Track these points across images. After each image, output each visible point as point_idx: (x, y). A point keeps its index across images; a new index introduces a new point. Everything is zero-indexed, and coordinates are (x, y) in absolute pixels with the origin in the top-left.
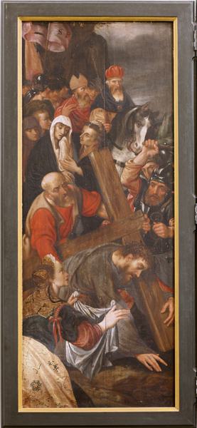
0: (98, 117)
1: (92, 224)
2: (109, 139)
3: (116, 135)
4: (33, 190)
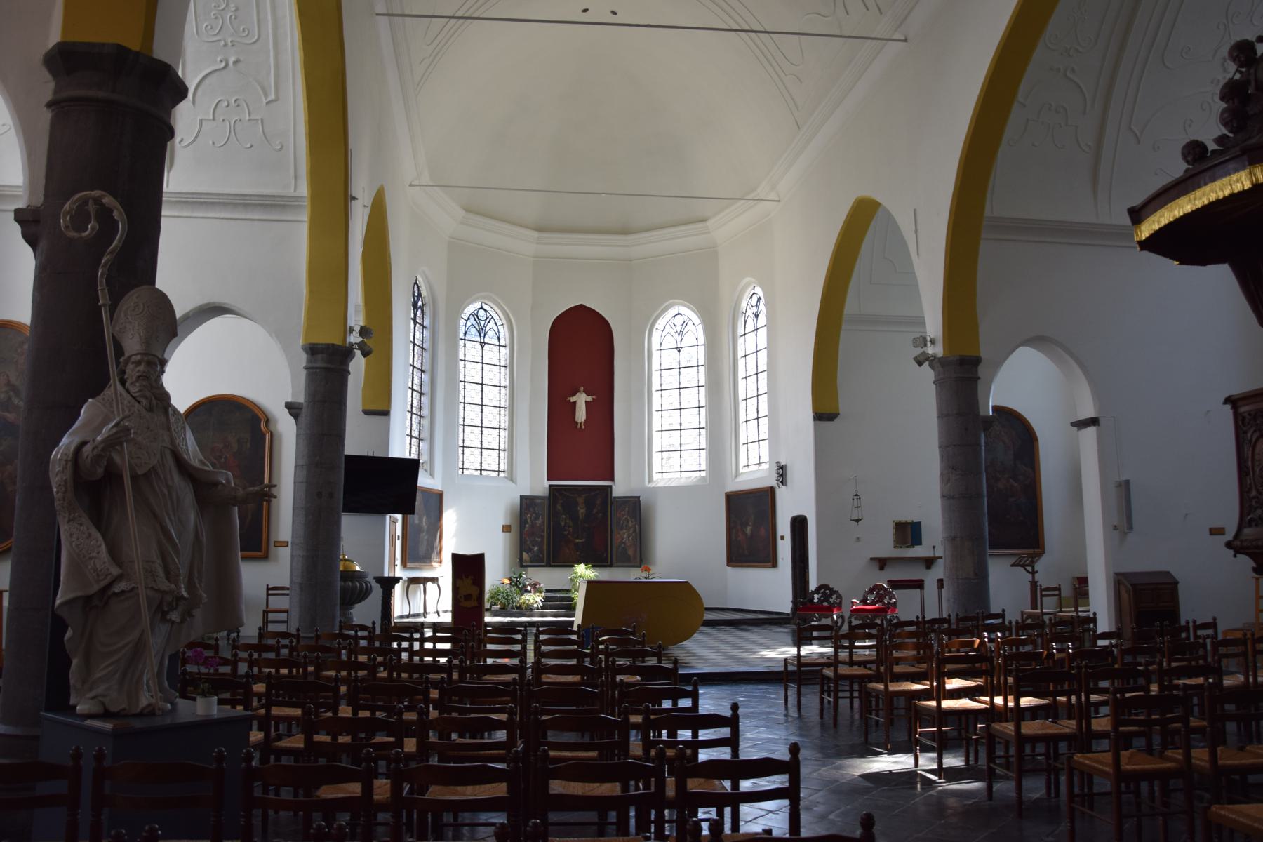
3: (537, 518)
4: (525, 527)
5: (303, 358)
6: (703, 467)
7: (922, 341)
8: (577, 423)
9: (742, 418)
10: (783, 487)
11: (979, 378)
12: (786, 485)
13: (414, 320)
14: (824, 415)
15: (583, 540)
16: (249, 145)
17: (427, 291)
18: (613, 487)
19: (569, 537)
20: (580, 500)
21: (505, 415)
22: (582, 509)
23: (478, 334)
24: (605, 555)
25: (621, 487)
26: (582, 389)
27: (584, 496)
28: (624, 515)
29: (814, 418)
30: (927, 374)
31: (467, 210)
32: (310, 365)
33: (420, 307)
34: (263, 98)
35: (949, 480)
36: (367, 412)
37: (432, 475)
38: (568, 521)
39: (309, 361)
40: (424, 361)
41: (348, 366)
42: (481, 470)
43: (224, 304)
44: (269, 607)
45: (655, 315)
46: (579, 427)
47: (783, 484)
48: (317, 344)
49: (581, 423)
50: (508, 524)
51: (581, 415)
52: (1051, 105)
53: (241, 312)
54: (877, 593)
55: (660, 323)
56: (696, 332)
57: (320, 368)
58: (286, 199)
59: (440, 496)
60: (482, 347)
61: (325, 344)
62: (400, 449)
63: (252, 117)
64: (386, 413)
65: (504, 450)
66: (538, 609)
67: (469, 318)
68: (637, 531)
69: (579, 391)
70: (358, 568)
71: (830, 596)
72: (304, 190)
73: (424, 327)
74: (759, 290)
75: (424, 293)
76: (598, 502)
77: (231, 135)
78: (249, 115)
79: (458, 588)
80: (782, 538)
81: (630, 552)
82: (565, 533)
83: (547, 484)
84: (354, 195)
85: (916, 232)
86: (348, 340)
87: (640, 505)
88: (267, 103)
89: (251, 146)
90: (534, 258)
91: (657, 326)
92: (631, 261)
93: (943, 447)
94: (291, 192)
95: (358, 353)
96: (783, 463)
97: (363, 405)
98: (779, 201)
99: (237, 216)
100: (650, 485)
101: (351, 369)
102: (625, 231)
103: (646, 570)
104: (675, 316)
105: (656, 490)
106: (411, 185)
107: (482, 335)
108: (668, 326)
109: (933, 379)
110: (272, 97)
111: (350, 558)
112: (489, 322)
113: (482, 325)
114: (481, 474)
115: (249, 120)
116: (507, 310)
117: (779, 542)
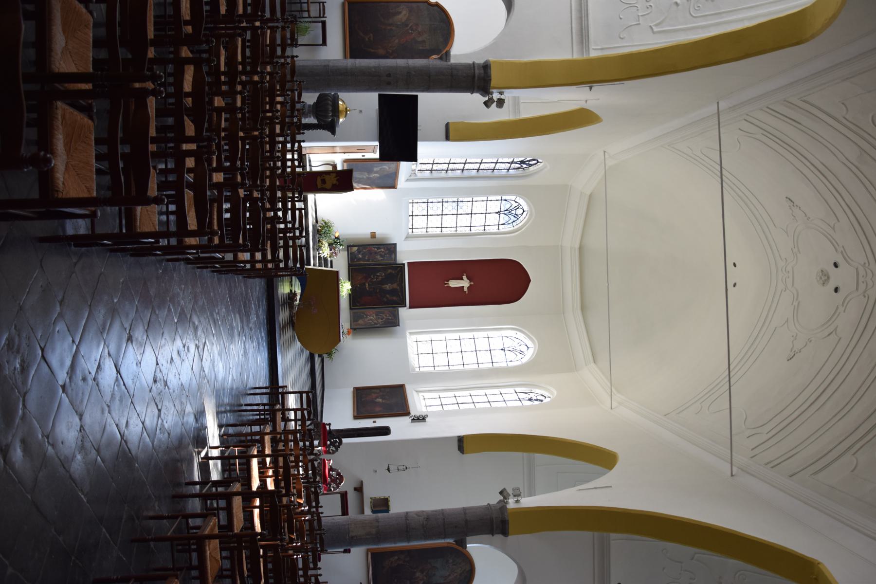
0: (383, 254)
1: (371, 254)
2: (381, 255)
3: (381, 256)
5: (480, 61)
6: (422, 369)
7: (517, 495)
8: (448, 281)
9: (457, 393)
10: (410, 420)
11: (493, 536)
12: (412, 422)
13: (512, 162)
14: (462, 443)
15: (367, 289)
16: (621, 17)
17: (533, 170)
18: (405, 308)
19: (370, 279)
20: (395, 286)
21: (451, 231)
22: (389, 287)
23: (506, 209)
24: (358, 304)
25: (405, 313)
26: (472, 283)
27: (398, 288)
28: (386, 316)
29: (460, 436)
30: (494, 499)
31: (590, 196)
32: (476, 65)
33: (522, 166)
34: (653, 24)
35: (419, 516)
36: (447, 126)
37: (407, 180)
38: (380, 278)
39: (479, 65)
40: (485, 171)
41: (477, 92)
42: (412, 216)
43: (514, 8)
44: (311, 4)
45: (526, 332)
46: (446, 282)
47: (412, 420)
48: (490, 69)
49: (448, 284)
50: (377, 236)
51: (453, 284)
52: (694, 579)
53: (509, 19)
54: (337, 478)
55: (521, 336)
56: (516, 361)
57: (474, 72)
58: (587, 43)
59: (393, 186)
60: (497, 213)
61: (490, 74)
62: (423, 149)
63: (641, 18)
64: (447, 138)
65: (427, 231)
66: (319, 254)
67: (516, 202)
68: (376, 326)
69: (470, 281)
70: (341, 120)
71: (334, 446)
72: (593, 54)
73: (508, 170)
74: (548, 400)
75: (531, 168)
76: (395, 298)
77: (625, 4)
78: (642, 16)
79: (330, 175)
80: (374, 422)
81: (361, 322)
82: (372, 277)
83: (405, 262)
84: (593, 88)
85: (595, 488)
86: (494, 91)
87: (394, 326)
88: (650, 26)
89: (621, 19)
90: (561, 246)
91: (519, 333)
92: (563, 314)
93: (442, 512)
94: (592, 46)
95: (486, 99)
96: (427, 419)
97: (453, 123)
98: (612, 409)
99: (574, 13)
100: (408, 334)
101: (474, 94)
102: (583, 308)
103: (348, 332)
104: (526, 345)
105: (405, 337)
106: (605, 152)
107: (506, 212)
108: (519, 341)
109: (491, 503)
110: (655, 29)
111: (348, 115)
112: (514, 217)
113: (512, 212)
114: (410, 216)
115: (638, 16)
116: (523, 229)
117: (372, 420)
